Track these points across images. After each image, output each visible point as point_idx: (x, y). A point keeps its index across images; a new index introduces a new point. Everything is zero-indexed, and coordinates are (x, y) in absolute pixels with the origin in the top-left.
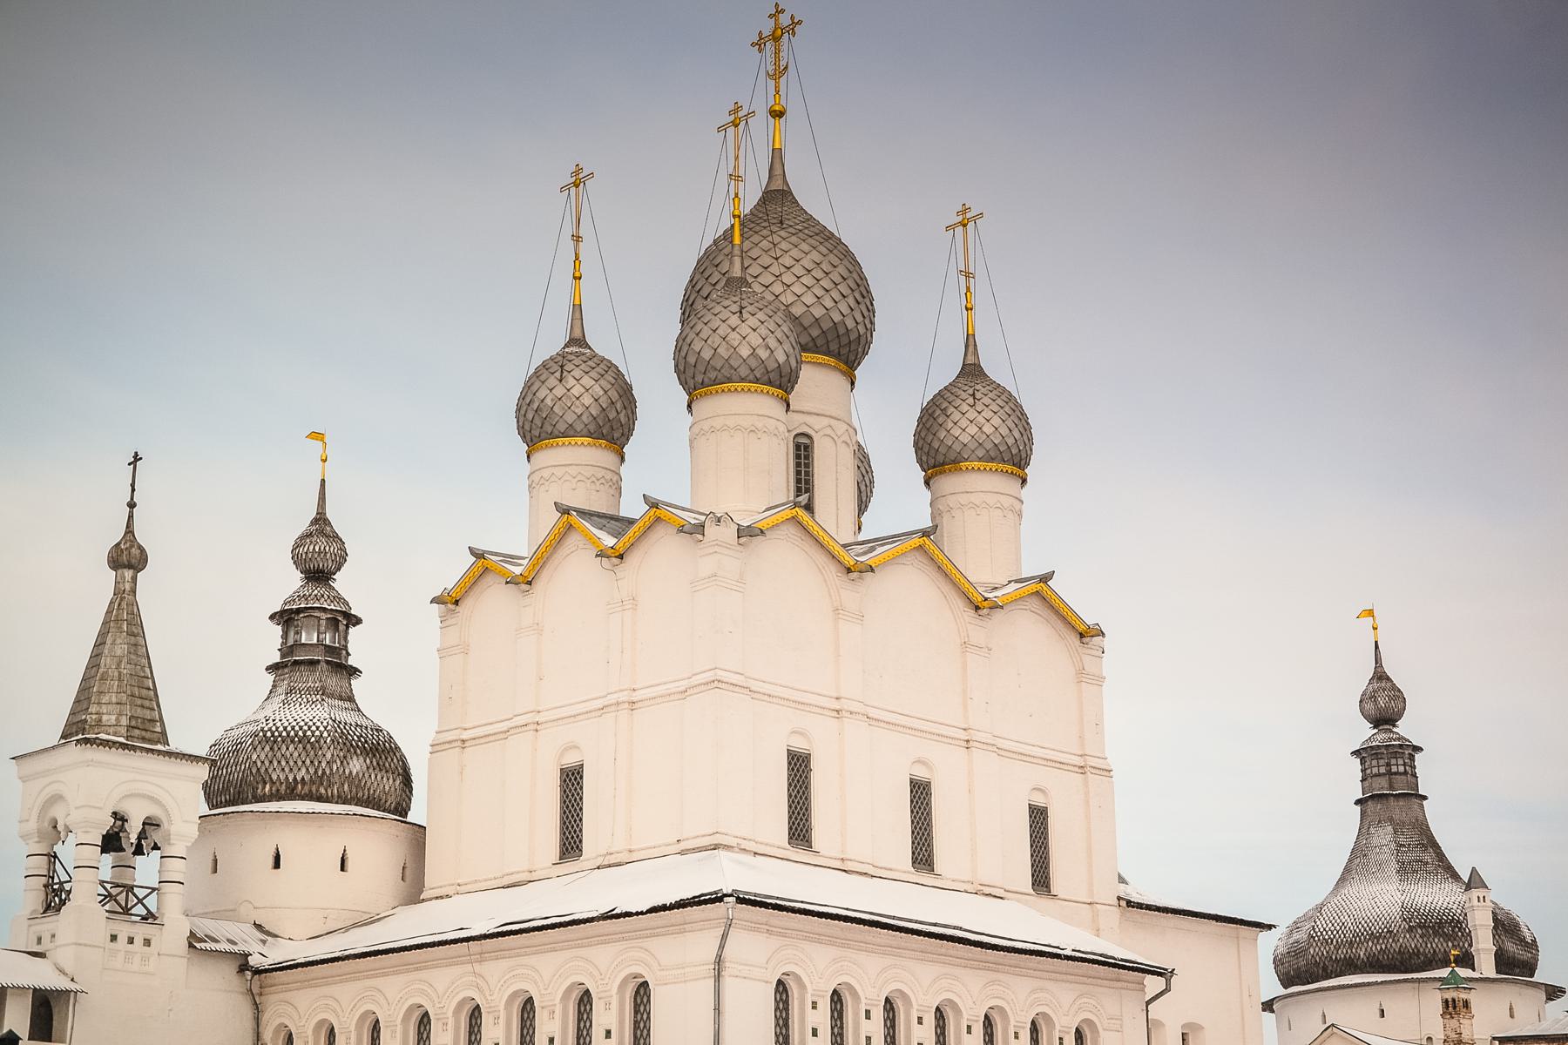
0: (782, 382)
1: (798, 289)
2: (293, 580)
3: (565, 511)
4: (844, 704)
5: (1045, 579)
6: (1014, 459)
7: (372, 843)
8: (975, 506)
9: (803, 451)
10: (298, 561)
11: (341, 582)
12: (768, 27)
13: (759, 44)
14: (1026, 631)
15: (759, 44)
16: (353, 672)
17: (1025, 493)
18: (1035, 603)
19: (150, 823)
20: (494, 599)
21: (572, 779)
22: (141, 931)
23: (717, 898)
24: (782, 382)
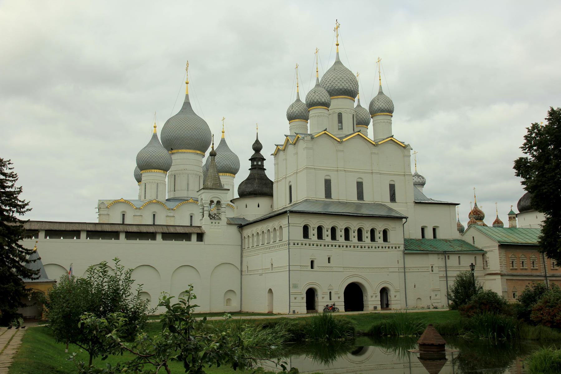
1: (336, 83)
2: (253, 152)
3: (287, 136)
4: (339, 169)
7: (263, 202)
8: (378, 123)
9: (340, 116)
10: (254, 149)
11: (262, 152)
12: (335, 26)
13: (335, 30)
14: (391, 148)
15: (335, 30)
16: (265, 169)
17: (392, 119)
19: (218, 202)
20: (281, 153)
21: (290, 187)
22: (217, 221)
23: (286, 212)
24: (326, 105)
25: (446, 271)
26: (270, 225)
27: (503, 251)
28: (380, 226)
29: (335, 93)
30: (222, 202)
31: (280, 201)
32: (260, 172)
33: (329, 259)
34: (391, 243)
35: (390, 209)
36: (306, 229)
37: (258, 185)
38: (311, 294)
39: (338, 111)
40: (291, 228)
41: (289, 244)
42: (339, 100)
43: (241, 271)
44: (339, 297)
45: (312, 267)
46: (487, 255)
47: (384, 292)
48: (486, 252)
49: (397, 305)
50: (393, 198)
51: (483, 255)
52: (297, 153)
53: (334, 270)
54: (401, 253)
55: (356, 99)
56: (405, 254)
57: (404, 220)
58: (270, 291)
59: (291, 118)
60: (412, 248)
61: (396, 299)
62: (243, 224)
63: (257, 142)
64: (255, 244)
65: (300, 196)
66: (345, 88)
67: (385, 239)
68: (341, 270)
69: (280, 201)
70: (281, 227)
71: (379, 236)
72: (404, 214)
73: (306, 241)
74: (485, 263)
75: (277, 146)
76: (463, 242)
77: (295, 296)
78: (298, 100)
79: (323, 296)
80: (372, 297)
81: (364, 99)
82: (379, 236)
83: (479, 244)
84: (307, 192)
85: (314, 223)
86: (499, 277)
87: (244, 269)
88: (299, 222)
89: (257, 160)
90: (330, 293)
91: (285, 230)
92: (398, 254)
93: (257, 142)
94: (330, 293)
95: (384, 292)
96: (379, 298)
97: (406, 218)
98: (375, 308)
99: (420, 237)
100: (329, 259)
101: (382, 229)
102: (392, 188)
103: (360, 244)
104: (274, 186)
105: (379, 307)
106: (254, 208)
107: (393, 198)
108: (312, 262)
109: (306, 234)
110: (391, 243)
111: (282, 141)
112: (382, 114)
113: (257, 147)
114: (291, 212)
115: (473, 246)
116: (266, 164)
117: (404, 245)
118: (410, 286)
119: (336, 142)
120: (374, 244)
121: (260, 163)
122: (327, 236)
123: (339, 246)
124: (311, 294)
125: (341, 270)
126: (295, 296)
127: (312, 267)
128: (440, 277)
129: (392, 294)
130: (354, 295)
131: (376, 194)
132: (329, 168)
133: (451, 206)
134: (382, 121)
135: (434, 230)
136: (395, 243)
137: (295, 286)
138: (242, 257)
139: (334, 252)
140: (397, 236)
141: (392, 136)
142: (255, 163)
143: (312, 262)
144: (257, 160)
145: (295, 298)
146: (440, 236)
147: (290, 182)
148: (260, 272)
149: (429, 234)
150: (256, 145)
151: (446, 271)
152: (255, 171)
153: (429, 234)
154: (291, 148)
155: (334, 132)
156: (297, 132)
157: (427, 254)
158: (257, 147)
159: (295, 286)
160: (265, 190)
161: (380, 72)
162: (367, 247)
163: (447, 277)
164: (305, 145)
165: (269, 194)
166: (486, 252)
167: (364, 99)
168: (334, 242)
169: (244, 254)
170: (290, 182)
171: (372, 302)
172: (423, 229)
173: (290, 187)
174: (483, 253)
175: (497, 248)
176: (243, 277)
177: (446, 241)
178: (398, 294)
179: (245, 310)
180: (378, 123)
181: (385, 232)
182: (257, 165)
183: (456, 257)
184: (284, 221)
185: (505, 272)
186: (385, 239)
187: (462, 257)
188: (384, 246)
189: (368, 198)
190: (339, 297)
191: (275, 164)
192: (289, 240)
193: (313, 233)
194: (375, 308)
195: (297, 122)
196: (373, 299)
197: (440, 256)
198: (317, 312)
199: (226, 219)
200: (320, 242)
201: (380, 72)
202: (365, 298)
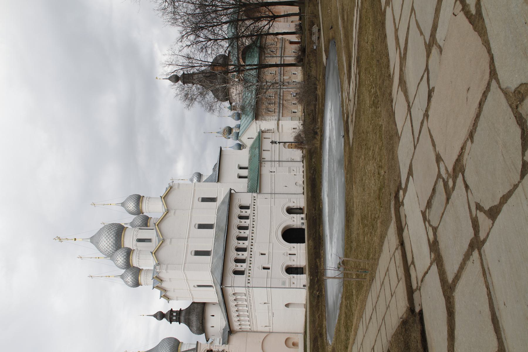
0: (129, 252)
2: (164, 320)
5: (161, 197)
6: (139, 199)
7: (210, 311)
8: (148, 208)
9: (139, 240)
10: (161, 319)
11: (165, 312)
13: (61, 242)
14: (171, 198)
15: (61, 242)
18: (166, 198)
20: (169, 294)
21: (199, 286)
23: (222, 289)
24: (129, 252)
25: (274, 161)
26: (232, 304)
27: (260, 118)
28: (236, 211)
29: (118, 244)
30: (208, 349)
31: (210, 296)
32: (183, 314)
33: (262, 254)
34: (250, 203)
35: (223, 202)
36: (236, 273)
37: (194, 316)
38: (290, 270)
39: (135, 242)
40: (236, 285)
41: (248, 287)
42: (125, 240)
43: (270, 332)
44: (294, 247)
45: (269, 269)
46: (263, 129)
47: (290, 211)
48: (261, 130)
49: (301, 202)
50: (213, 200)
51: (263, 132)
52: (170, 279)
53: (271, 250)
54: (259, 195)
55: (125, 226)
56: (260, 192)
57: (232, 191)
58: (287, 305)
59: (137, 284)
60: (256, 186)
61: (295, 202)
62: (228, 330)
63: (155, 316)
64: (247, 318)
65: (207, 277)
66: (115, 234)
67: (248, 208)
68: (271, 244)
69: (210, 296)
70: (234, 294)
71: (244, 213)
72: (228, 191)
73: (247, 272)
74: (268, 131)
75: (161, 297)
76: (252, 147)
77: (292, 283)
78: (122, 277)
79: (292, 260)
80: (294, 221)
81: (126, 219)
82: (244, 213)
83: (255, 135)
84: (204, 272)
85: (232, 266)
86: (280, 122)
87: (267, 329)
88: (231, 278)
89: (172, 316)
90: (290, 254)
91: (237, 290)
92: (260, 198)
93: (155, 316)
94: (290, 254)
95: (290, 211)
96: (295, 215)
97: (231, 190)
98: (302, 219)
99: (246, 179)
100: (262, 254)
101: (239, 210)
102: (204, 200)
103: (250, 228)
104: (196, 301)
105: (303, 216)
106: (216, 321)
107: (213, 200)
108: (264, 268)
109: (242, 273)
110: (250, 203)
111: (158, 292)
112: (140, 204)
113: (160, 316)
114: (222, 284)
115: (256, 139)
116: (176, 308)
117: (252, 192)
118: (285, 190)
119: (163, 244)
120: (251, 217)
121: (175, 314)
122: (243, 255)
123: (252, 245)
124: (290, 270)
125: (271, 244)
126: (292, 283)
127: (269, 269)
128: (279, 166)
129: (292, 205)
130: (291, 235)
131: (210, 214)
132: (185, 251)
133: (222, 154)
134: (147, 204)
135: (241, 168)
136: (250, 201)
137: (284, 283)
138: (257, 332)
139: (256, 250)
140: (246, 199)
141: (161, 197)
142: (174, 318)
143: (264, 268)
144: (172, 316)
145: (294, 283)
146: (246, 164)
147: (194, 286)
148: (271, 314)
149: (245, 173)
150: (158, 317)
151: (274, 161)
152: (182, 318)
153: (245, 173)
154: (164, 285)
155: (152, 246)
156: (152, 278)
157: (260, 175)
158: (160, 316)
159: (284, 283)
160: (199, 309)
161: (104, 205)
162: (253, 223)
163: (279, 161)
164: (164, 271)
165: (204, 305)
166: (261, 130)
167: (126, 219)
168: (249, 250)
169: (255, 330)
170: (194, 286)
171: (297, 221)
172: (240, 177)
173: (199, 286)
174: (261, 133)
175: (258, 122)
176: (274, 331)
177: (250, 160)
178: (292, 200)
179: (302, 331)
180: (148, 208)
181: (242, 207)
182: (175, 316)
183: (264, 153)
184: (230, 291)
185: (276, 118)
186: (248, 208)
187: (264, 148)
188: (253, 209)
189: (212, 220)
190: (294, 247)
191: (177, 300)
192: (245, 287)
193: (240, 267)
194: (302, 219)
195: (142, 278)
196: (295, 220)
197: (263, 165)
198: (305, 266)
199: (224, 345)
200: (248, 261)
201: (104, 205)
202: (295, 227)
